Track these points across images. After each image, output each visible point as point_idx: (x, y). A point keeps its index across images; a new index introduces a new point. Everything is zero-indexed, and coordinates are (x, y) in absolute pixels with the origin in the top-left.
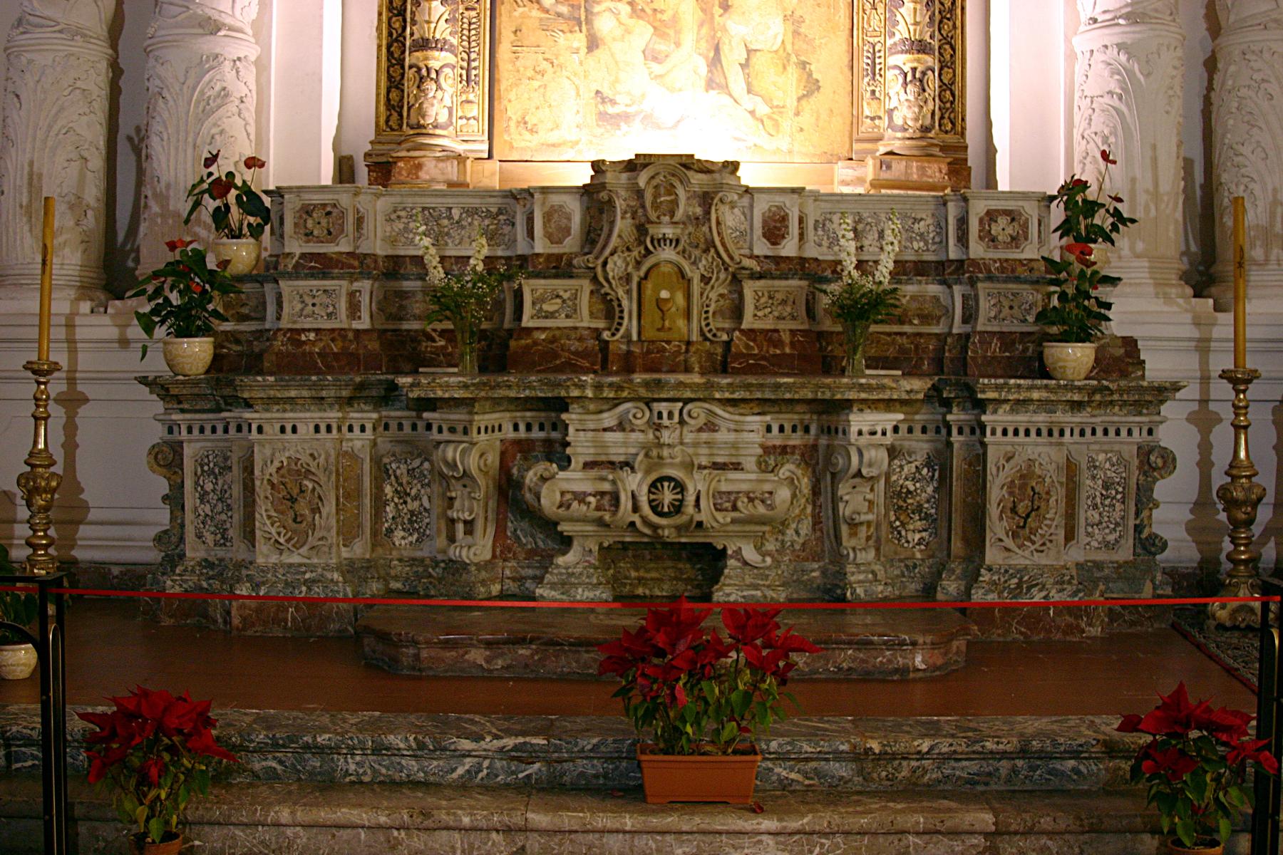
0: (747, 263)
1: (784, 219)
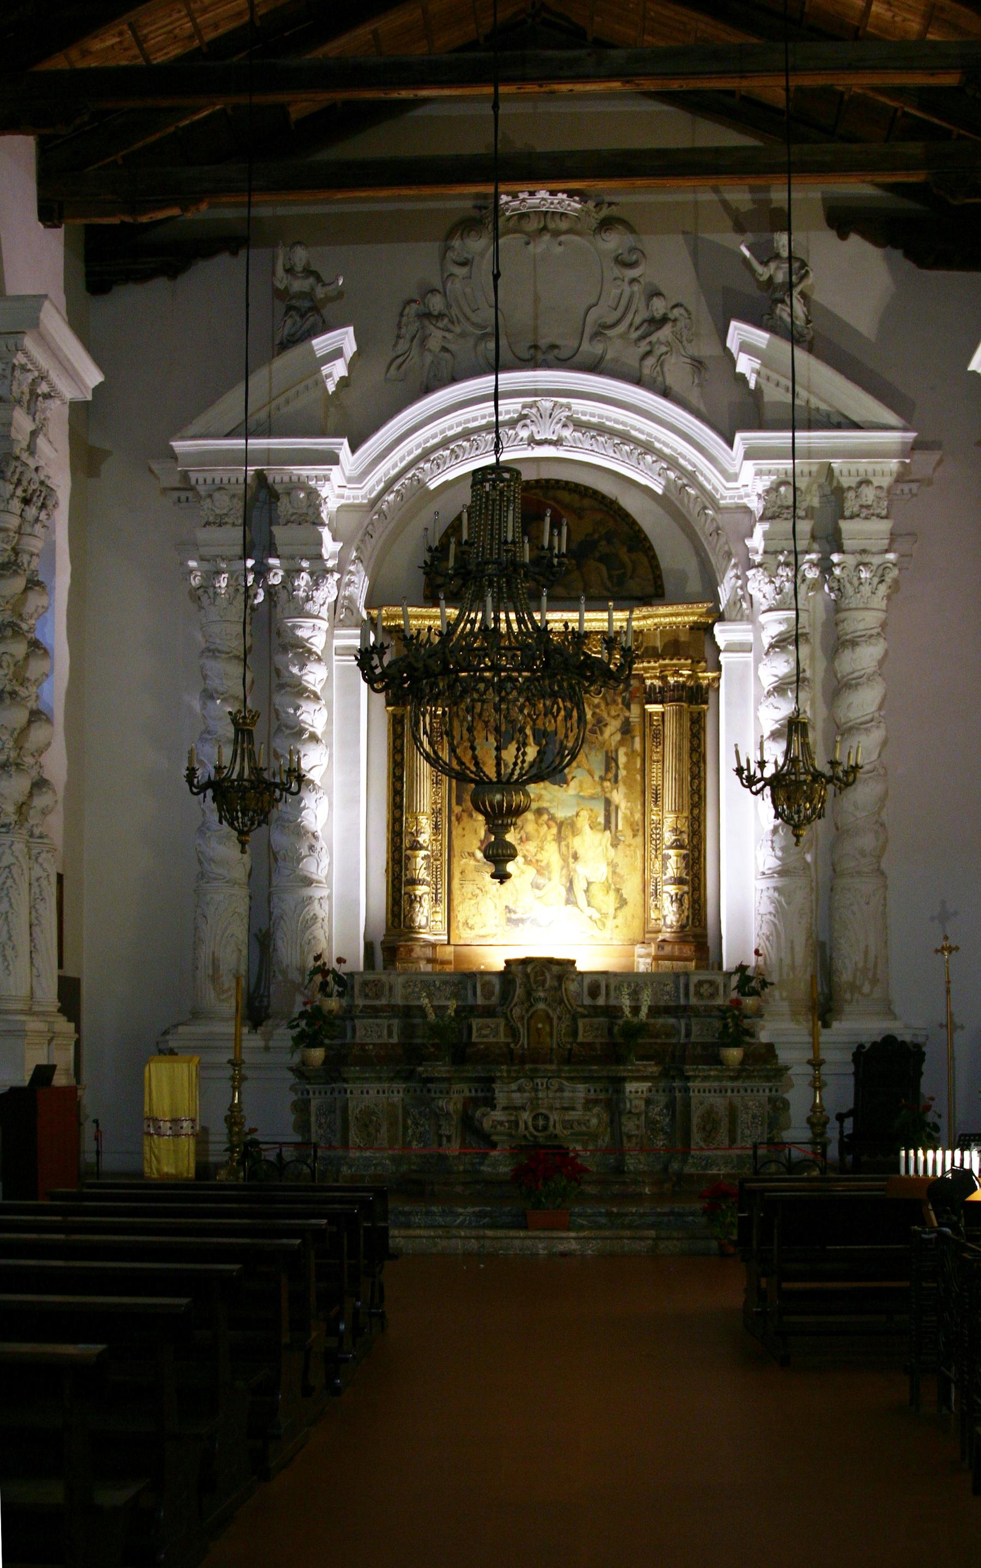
0: (579, 1010)
1: (598, 987)
